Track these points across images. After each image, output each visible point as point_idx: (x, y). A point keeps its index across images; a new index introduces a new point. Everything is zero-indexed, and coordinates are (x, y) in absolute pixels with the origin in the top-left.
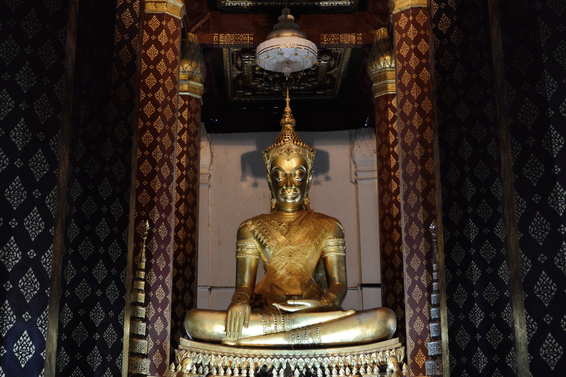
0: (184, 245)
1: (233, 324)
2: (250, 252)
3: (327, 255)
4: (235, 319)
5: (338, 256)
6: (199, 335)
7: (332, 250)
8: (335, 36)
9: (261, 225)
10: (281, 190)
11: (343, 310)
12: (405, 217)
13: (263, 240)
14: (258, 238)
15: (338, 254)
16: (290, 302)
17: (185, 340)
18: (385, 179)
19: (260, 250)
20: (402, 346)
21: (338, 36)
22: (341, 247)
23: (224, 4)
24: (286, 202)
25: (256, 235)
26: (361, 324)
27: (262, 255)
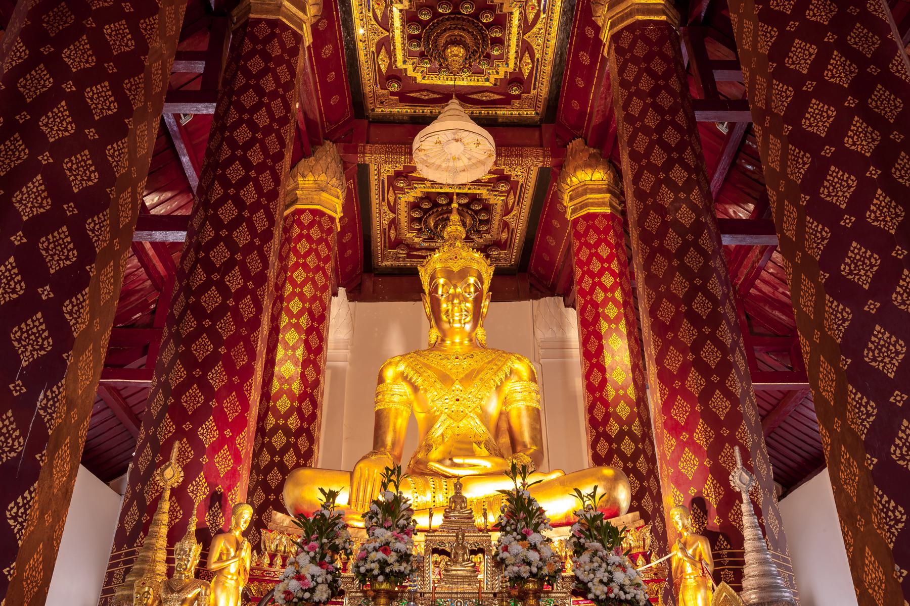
1: (362, 488)
5: (528, 407)
8: (517, 150)
18: (590, 319)
19: (412, 397)
21: (521, 150)
23: (373, 110)
24: (452, 327)
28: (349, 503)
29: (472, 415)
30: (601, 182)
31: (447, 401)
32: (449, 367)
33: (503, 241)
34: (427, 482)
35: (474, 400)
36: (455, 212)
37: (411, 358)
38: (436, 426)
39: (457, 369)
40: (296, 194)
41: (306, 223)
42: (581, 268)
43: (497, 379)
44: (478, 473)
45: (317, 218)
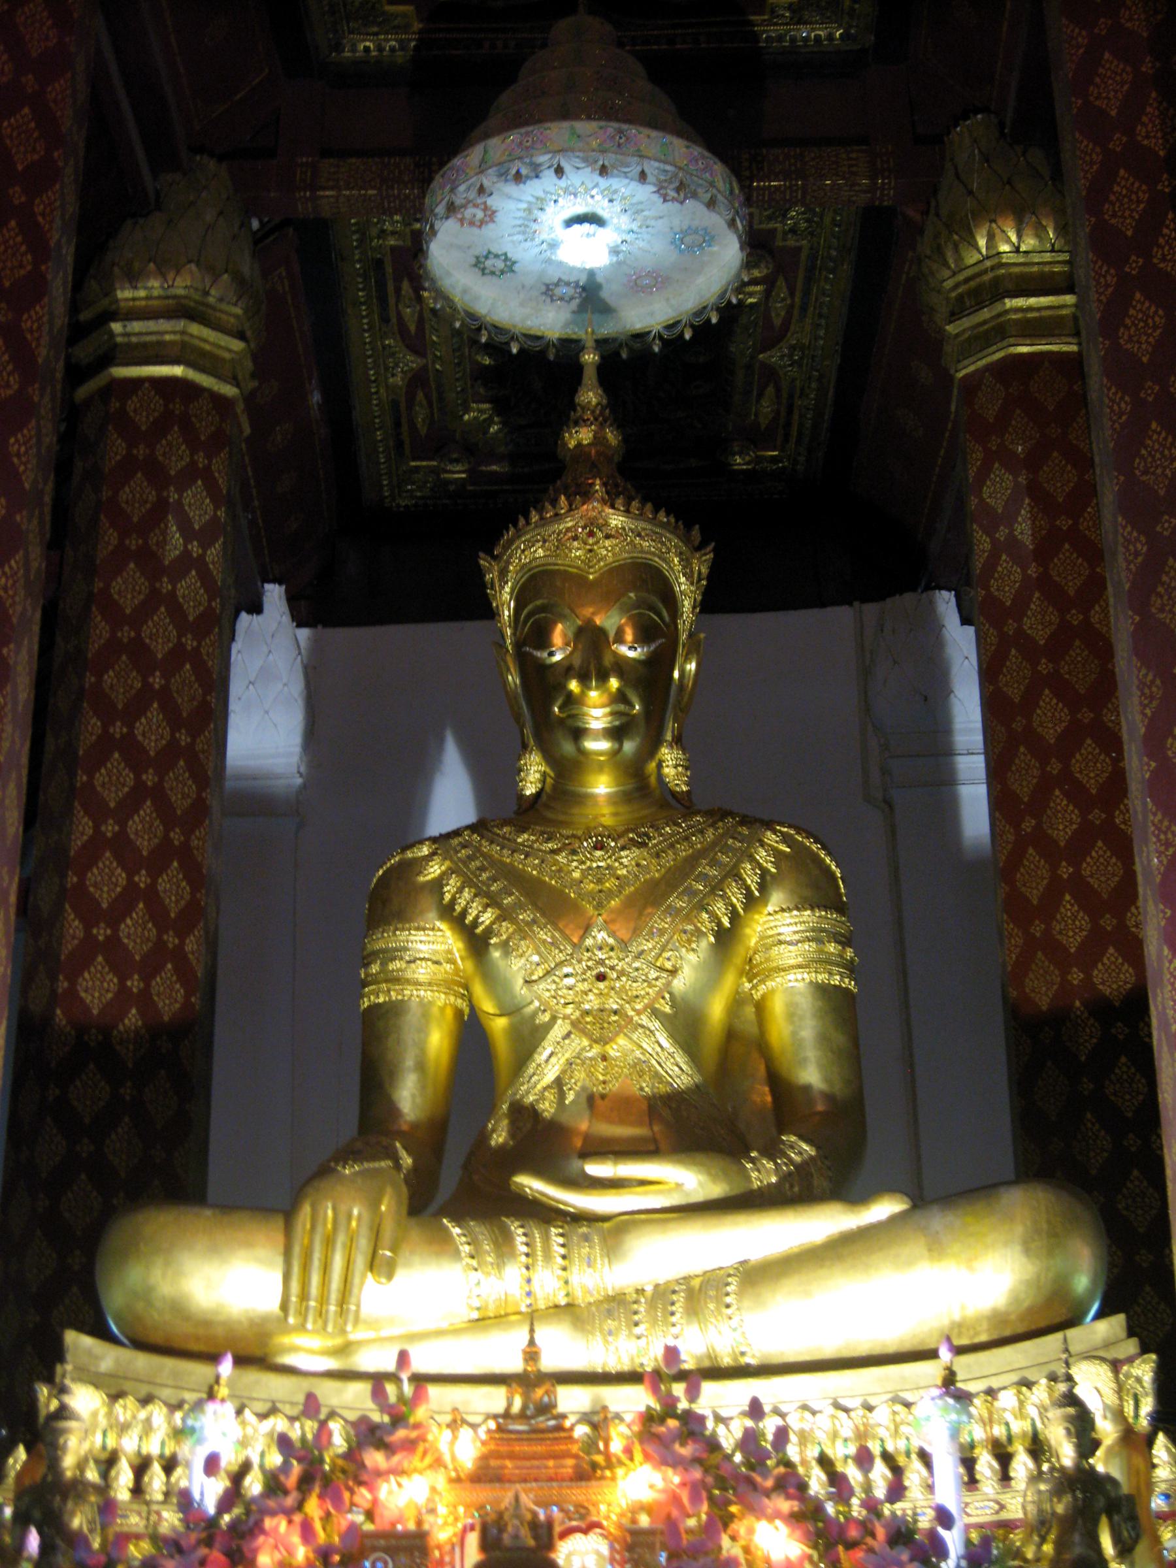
0: (147, 979)
2: (422, 972)
3: (770, 984)
4: (329, 1243)
6: (158, 1321)
7: (793, 962)
9: (471, 858)
10: (559, 702)
11: (856, 1197)
12: (1142, 685)
13: (477, 917)
14: (458, 908)
15: (822, 977)
16: (595, 1169)
17: (87, 1341)
19: (467, 966)
20: (1145, 1349)
22: (832, 948)
24: (582, 752)
25: (448, 897)
26: (936, 1248)
27: (478, 990)
28: (284, 1307)
29: (644, 1020)
30: (1048, 257)
31: (570, 981)
32: (576, 875)
33: (764, 422)
34: (508, 1238)
35: (653, 974)
36: (590, 376)
37: (464, 847)
38: (541, 1056)
39: (600, 881)
40: (112, 334)
41: (143, 421)
42: (990, 532)
43: (719, 908)
44: (658, 1206)
45: (177, 407)
